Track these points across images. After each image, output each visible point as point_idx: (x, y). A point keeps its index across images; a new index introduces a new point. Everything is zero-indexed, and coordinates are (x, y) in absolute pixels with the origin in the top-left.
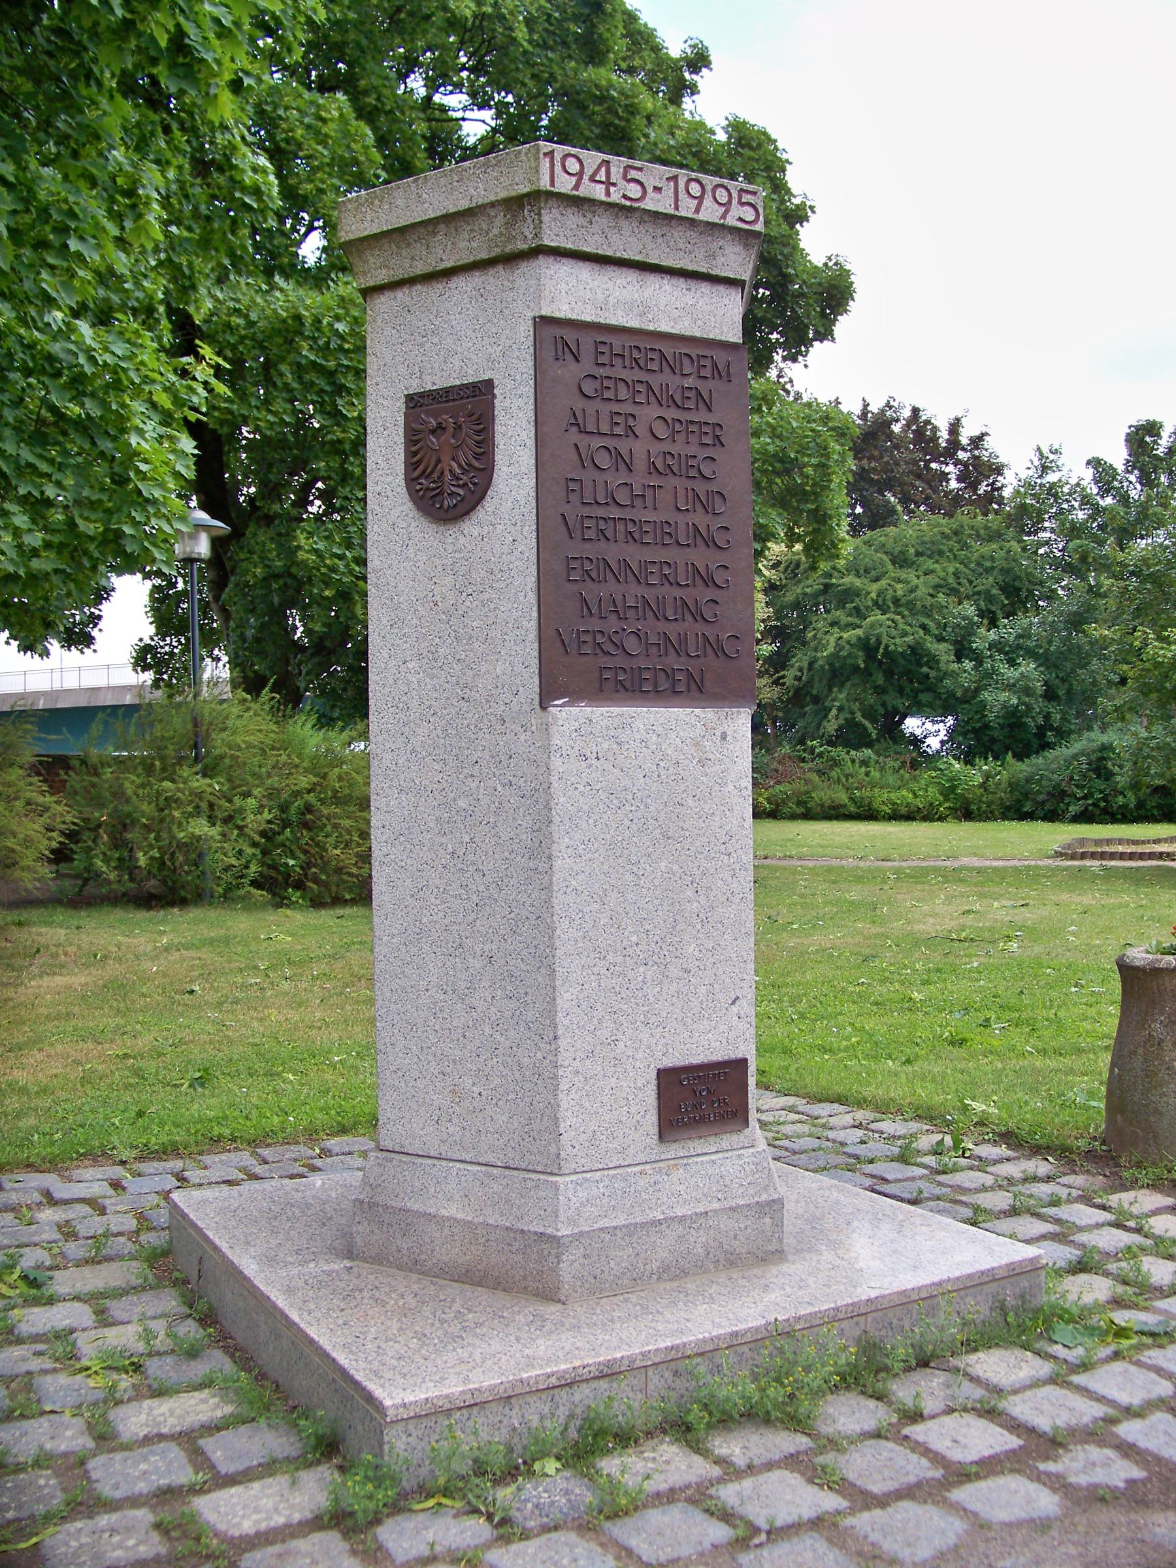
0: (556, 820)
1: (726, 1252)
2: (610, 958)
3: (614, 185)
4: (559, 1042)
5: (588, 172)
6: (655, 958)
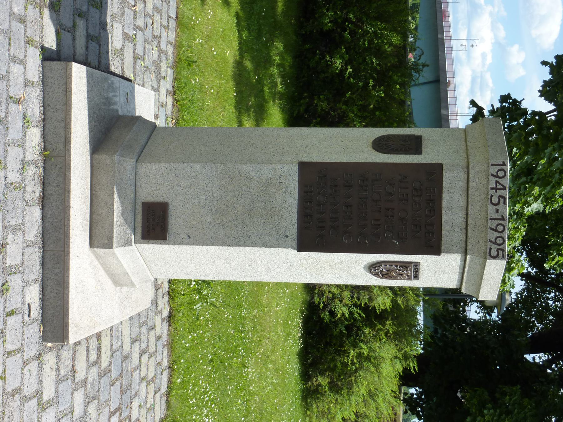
0: (259, 166)
1: (98, 223)
2: (209, 185)
3: (496, 192)
4: (182, 164)
5: (500, 180)
6: (208, 203)
